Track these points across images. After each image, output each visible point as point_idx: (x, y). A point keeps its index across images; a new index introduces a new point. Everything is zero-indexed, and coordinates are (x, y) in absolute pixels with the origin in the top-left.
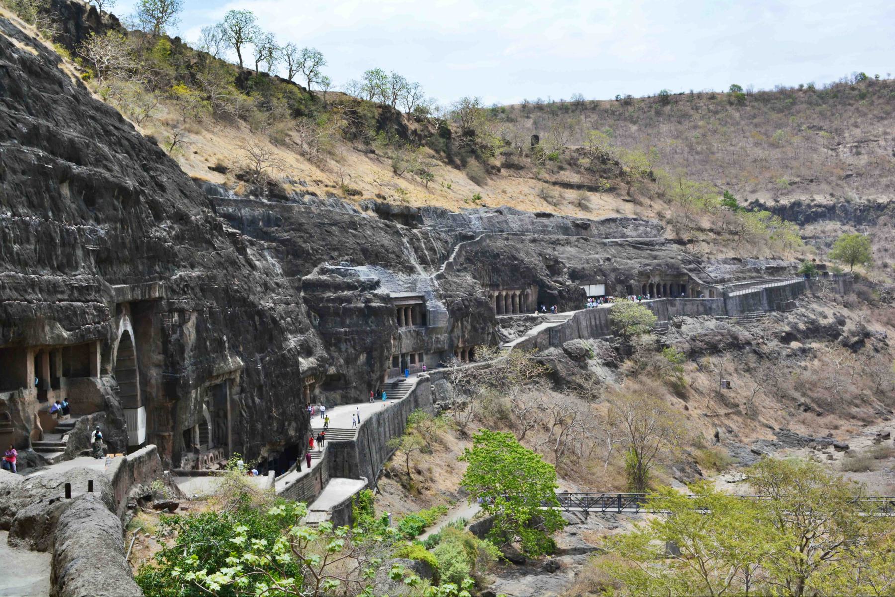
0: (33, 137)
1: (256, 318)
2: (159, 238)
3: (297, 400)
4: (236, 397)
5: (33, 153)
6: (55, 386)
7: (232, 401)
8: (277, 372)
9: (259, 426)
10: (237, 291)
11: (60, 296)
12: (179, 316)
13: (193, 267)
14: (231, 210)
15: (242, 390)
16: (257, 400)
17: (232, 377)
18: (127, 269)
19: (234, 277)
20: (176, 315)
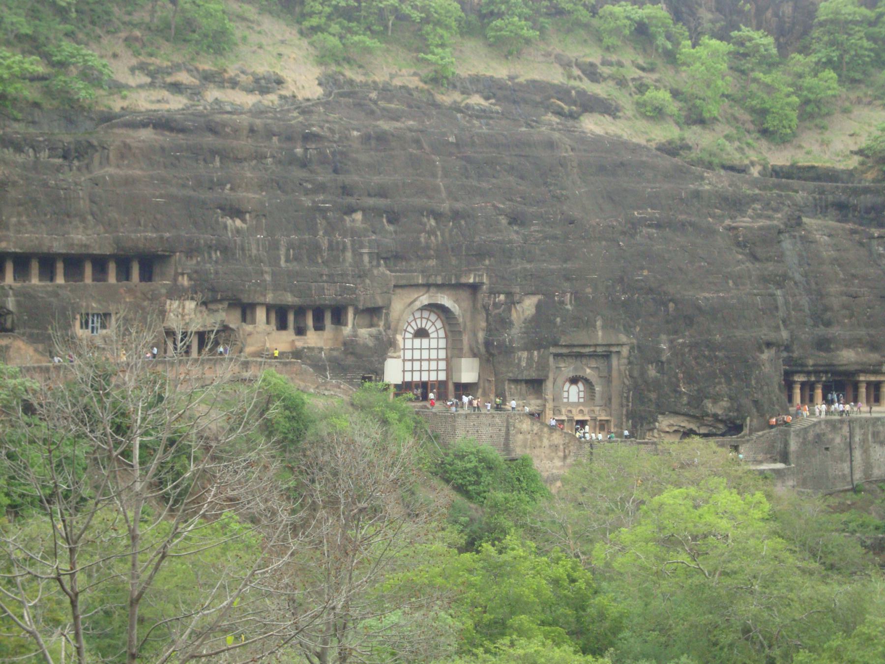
0: (321, 188)
1: (671, 305)
2: (497, 242)
3: (735, 384)
4: (622, 368)
5: (306, 201)
6: (319, 326)
7: (619, 370)
8: (695, 353)
9: (653, 396)
10: (637, 280)
11: (299, 279)
12: (506, 297)
13: (565, 261)
14: (844, 198)
15: (630, 363)
16: (652, 372)
17: (614, 349)
18: (432, 262)
19: (642, 268)
20: (502, 297)
